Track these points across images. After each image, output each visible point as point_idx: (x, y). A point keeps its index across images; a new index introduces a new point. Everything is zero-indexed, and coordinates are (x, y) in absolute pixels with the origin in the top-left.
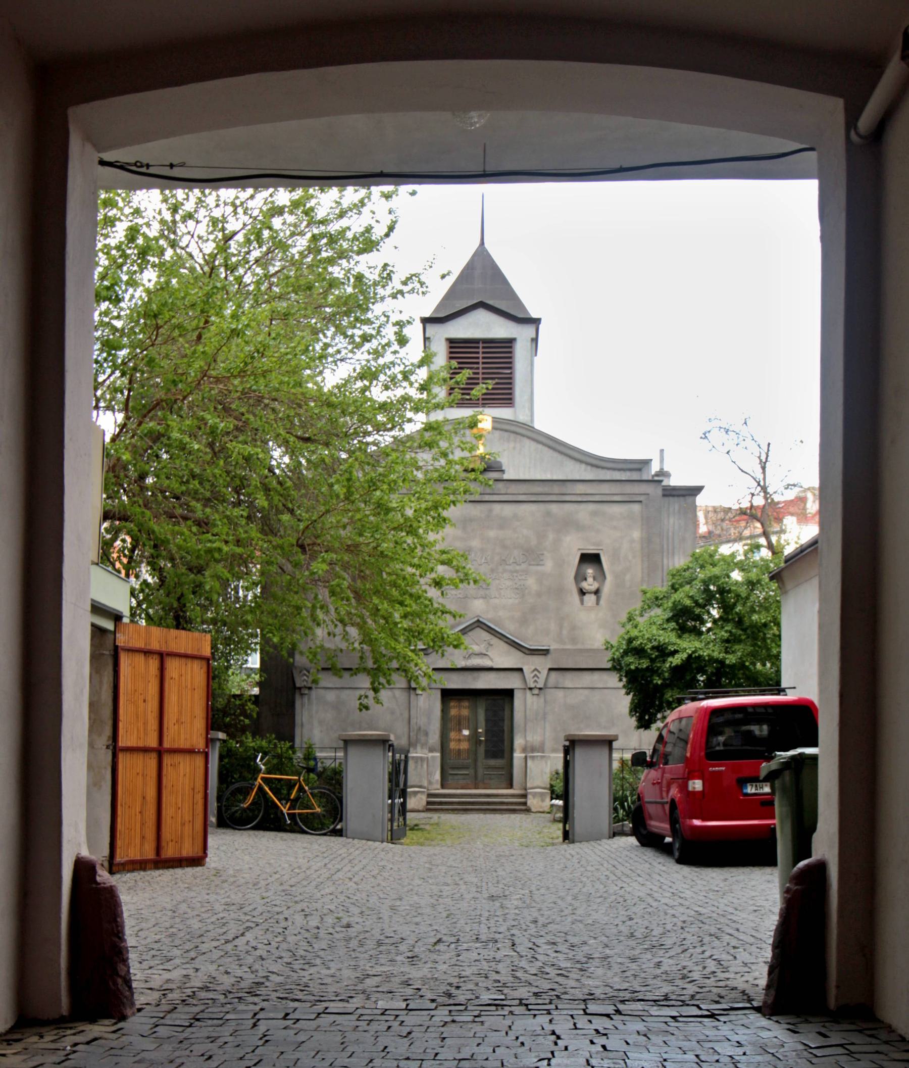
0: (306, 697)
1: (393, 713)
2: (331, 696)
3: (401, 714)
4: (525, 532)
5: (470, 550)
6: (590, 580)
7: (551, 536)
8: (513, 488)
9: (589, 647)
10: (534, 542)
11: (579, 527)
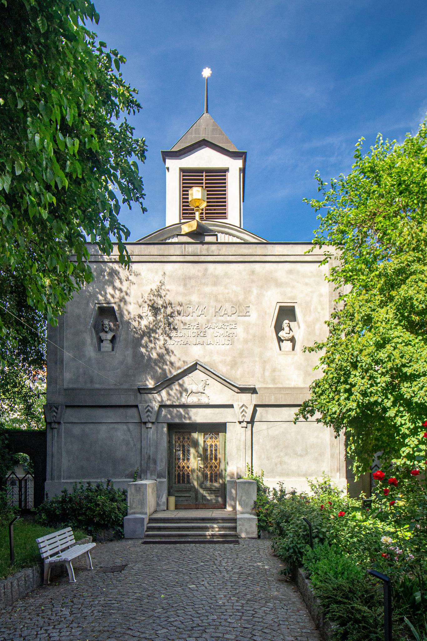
0: (56, 430)
1: (128, 444)
2: (77, 430)
3: (135, 445)
4: (234, 287)
5: (190, 303)
6: (287, 329)
7: (255, 291)
8: (224, 250)
9: (287, 386)
10: (241, 298)
11: (278, 284)
